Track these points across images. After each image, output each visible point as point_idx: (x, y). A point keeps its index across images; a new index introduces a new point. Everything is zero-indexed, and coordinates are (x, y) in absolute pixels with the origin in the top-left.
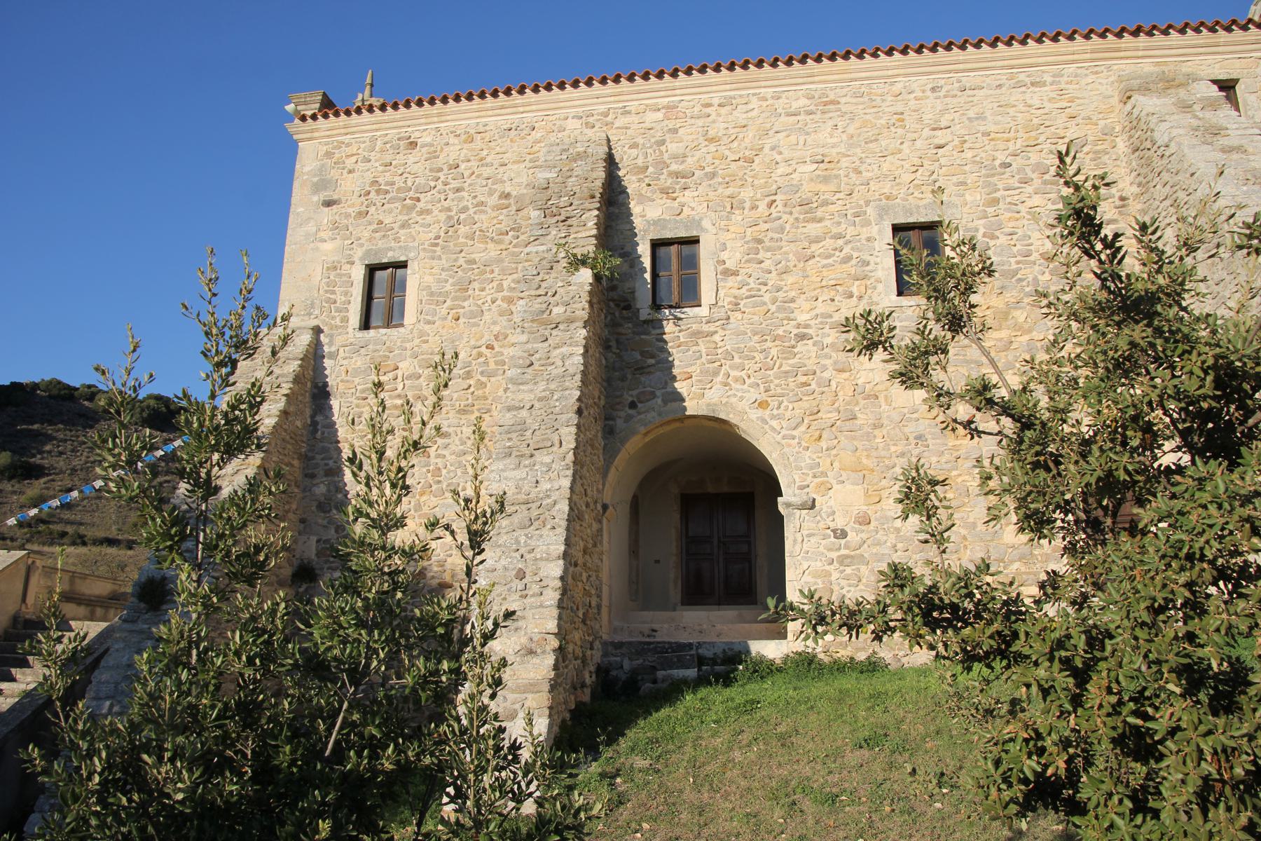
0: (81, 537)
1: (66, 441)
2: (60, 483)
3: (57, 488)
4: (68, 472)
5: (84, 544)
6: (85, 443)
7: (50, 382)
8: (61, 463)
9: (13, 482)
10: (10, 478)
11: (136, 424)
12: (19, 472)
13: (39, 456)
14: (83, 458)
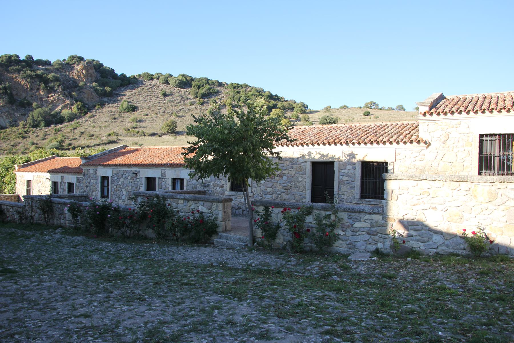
0: (144, 133)
2: (144, 112)
3: (143, 114)
4: (147, 108)
5: (145, 136)
6: (154, 96)
7: (144, 74)
8: (145, 105)
9: (128, 113)
10: (128, 112)
12: (130, 109)
13: (138, 103)
14: (153, 102)
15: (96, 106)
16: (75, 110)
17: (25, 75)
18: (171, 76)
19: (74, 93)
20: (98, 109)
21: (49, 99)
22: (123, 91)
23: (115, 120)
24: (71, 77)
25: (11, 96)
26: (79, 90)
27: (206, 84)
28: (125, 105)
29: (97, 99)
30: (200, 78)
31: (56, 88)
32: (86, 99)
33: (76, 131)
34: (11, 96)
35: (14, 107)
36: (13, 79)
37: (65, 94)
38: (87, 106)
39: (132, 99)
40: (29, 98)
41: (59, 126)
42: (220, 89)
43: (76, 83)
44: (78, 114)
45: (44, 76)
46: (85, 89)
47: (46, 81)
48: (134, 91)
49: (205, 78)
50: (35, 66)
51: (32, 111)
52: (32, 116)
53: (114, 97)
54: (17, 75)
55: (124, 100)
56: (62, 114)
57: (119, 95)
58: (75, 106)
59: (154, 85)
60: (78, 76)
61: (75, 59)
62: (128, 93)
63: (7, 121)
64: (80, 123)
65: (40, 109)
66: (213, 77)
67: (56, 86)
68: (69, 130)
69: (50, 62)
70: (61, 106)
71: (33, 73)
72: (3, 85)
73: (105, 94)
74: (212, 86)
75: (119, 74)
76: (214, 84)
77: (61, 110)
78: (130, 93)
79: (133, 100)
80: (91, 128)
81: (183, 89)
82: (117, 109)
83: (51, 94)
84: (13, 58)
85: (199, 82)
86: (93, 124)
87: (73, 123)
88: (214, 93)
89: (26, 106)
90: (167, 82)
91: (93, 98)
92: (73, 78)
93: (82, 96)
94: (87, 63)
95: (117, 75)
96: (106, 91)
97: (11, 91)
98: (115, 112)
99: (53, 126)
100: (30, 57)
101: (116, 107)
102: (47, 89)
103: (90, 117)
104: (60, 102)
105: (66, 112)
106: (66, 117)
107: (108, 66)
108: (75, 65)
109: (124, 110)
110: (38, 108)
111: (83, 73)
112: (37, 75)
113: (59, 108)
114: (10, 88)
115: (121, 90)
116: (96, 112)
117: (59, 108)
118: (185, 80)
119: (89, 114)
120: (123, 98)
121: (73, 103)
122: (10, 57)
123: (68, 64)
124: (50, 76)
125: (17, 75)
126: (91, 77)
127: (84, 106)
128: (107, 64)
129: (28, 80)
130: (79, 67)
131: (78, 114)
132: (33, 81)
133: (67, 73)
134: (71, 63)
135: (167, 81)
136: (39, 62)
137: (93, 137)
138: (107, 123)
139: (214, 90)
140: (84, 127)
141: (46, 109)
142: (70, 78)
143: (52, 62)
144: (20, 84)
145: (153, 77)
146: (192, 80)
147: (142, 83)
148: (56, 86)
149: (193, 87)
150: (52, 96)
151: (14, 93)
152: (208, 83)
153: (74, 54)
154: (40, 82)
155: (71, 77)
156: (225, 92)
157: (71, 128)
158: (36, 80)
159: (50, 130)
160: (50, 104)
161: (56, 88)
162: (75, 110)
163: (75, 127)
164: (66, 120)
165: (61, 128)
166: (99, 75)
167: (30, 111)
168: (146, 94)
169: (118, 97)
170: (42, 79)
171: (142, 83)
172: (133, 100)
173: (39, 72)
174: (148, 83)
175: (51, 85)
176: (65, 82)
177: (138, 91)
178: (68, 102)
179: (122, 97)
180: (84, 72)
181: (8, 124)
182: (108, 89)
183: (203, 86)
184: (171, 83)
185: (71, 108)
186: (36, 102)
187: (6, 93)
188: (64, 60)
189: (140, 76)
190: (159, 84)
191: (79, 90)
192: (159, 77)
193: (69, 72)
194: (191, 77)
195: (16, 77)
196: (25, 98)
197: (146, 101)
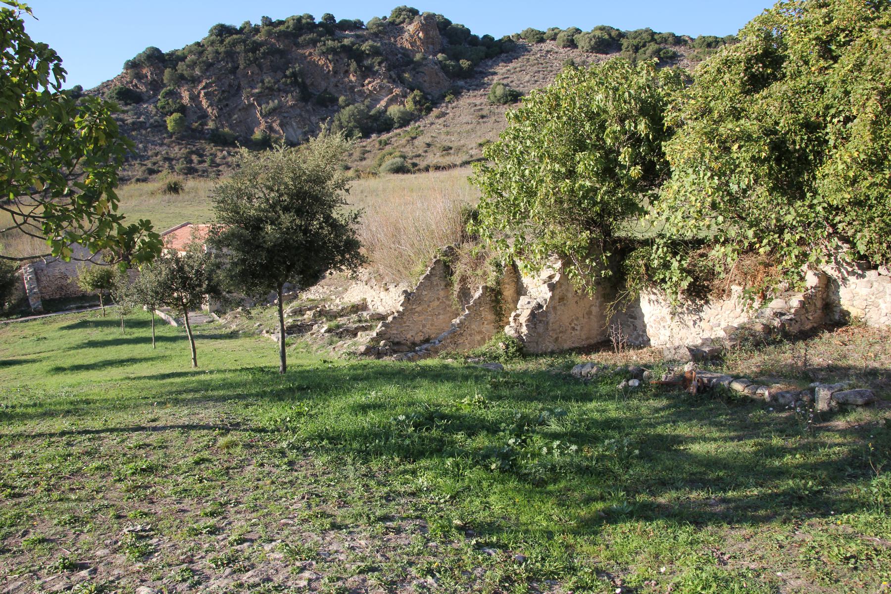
1: (539, 72)
7: (527, 31)
10: (505, 103)
11: (587, 51)
12: (509, 98)
15: (445, 96)
16: (409, 105)
17: (324, 49)
18: (578, 31)
19: (406, 75)
20: (449, 102)
21: (365, 88)
22: (491, 67)
23: (484, 120)
24: (399, 46)
25: (303, 88)
26: (414, 69)
27: (649, 42)
28: (499, 91)
29: (447, 84)
30: (636, 32)
31: (377, 68)
32: (426, 85)
33: (416, 142)
34: (303, 88)
35: (309, 107)
36: (306, 57)
37: (391, 77)
38: (429, 97)
39: (510, 80)
40: (333, 90)
41: (384, 136)
42: (680, 50)
43: (408, 56)
44: (416, 113)
45: (355, 47)
46: (425, 65)
47: (359, 56)
48: (511, 66)
49: (647, 31)
50: (338, 32)
51: (338, 111)
52: (339, 120)
53: (476, 79)
54: (312, 51)
55: (495, 82)
56: (388, 113)
57: (487, 74)
58: (410, 98)
59: (548, 52)
60: (411, 43)
61: (404, 13)
62: (501, 69)
63: (299, 131)
64: (422, 128)
65: (351, 107)
66: (662, 28)
67: (376, 64)
68: (403, 141)
69: (362, 24)
70: (386, 99)
71: (336, 44)
72: (291, 70)
73: (460, 74)
74: (662, 46)
75: (481, 36)
76: (665, 40)
77: (386, 107)
78: (504, 70)
79: (512, 82)
80: (443, 136)
81: (604, 56)
82: (484, 100)
83: (369, 79)
84: (304, 21)
85: (635, 38)
86: (444, 130)
87: (408, 128)
88: (667, 58)
89: (328, 104)
90: (571, 43)
91: (439, 83)
92: (402, 48)
93: (420, 80)
94: (425, 19)
95: (476, 37)
96: (462, 68)
97: (303, 79)
98: (481, 104)
99: (374, 136)
100: (330, 18)
101: (481, 95)
102: (361, 71)
103: (438, 117)
104: (383, 92)
105: (394, 110)
106: (395, 120)
107: (460, 23)
108: (404, 25)
109: (499, 100)
110: (348, 105)
111: (420, 38)
112: (343, 47)
113: (383, 103)
114: (301, 72)
115: (487, 66)
116: (447, 107)
117: (383, 103)
118: (607, 37)
119: (435, 112)
120: (493, 80)
121: (406, 92)
122: (299, 19)
123: (392, 23)
124: (365, 47)
125: (312, 51)
126: (433, 44)
127: (424, 97)
128: (456, 20)
129: (330, 57)
130: (411, 28)
131: (416, 113)
132: (338, 58)
133: (392, 40)
134: (398, 21)
135: (572, 41)
136: (346, 25)
137: (452, 151)
138: (470, 127)
139: (668, 52)
140: (429, 135)
141: (362, 108)
142: (397, 49)
143: (365, 23)
144: (317, 65)
145: (545, 36)
146: (621, 35)
147: (525, 49)
148: (376, 64)
149: (624, 49)
150: (370, 83)
151: (308, 82)
152: (653, 40)
153: (401, 5)
154: (349, 58)
155: (399, 46)
156: (691, 56)
157: (408, 138)
158: (342, 55)
159: (370, 143)
160: (366, 98)
161: (377, 68)
162: (409, 105)
163: (413, 135)
164: (396, 125)
165: (388, 139)
166: (445, 41)
167: (335, 111)
168: (535, 68)
169: (483, 78)
170: (352, 53)
171: (525, 49)
172: (512, 82)
173: (346, 42)
174: (535, 48)
175: (367, 62)
176: (390, 57)
177: (519, 65)
178: (397, 91)
179: (490, 77)
180: (421, 35)
181: (300, 137)
182: (465, 63)
183: (644, 46)
184: (581, 44)
185: (402, 103)
186: (343, 95)
187: (295, 83)
188: (385, 18)
189: (519, 36)
190: (557, 50)
191: (414, 69)
192: (556, 34)
193: (395, 38)
194: (618, 30)
195: (310, 54)
196: (326, 90)
197: (536, 81)
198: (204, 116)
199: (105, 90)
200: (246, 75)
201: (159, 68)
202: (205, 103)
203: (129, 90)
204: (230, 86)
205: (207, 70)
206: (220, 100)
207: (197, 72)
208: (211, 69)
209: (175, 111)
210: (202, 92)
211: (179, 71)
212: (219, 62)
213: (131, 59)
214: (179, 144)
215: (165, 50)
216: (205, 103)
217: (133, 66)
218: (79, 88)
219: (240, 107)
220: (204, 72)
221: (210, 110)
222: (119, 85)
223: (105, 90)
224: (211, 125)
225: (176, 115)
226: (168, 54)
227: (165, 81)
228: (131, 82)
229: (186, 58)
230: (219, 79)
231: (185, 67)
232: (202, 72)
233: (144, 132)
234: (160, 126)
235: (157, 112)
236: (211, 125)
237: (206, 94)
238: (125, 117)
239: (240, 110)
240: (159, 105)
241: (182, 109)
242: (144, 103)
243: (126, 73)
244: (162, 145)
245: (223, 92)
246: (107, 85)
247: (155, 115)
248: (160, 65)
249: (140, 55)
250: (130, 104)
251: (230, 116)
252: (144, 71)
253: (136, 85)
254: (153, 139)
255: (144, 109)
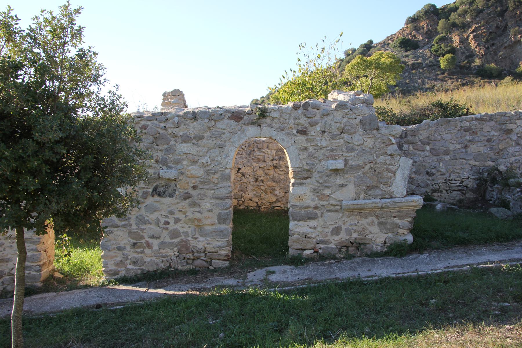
198: (471, 55)
199: (390, 42)
200: (514, 16)
201: (433, 20)
202: (473, 44)
203: (408, 40)
204: (497, 27)
205: (476, 16)
206: (487, 41)
207: (468, 18)
208: (481, 14)
209: (446, 53)
210: (472, 35)
211: (451, 21)
212: (488, 7)
213: (411, 15)
214: (451, 78)
215: (439, 6)
216: (473, 44)
217: (413, 20)
218: (371, 42)
219: (506, 45)
220: (473, 18)
221: (477, 49)
222: (400, 37)
223: (390, 42)
224: (478, 62)
225: (448, 56)
226: (441, 9)
227: (439, 29)
228: (411, 34)
229: (457, 8)
230: (487, 23)
231: (457, 16)
232: (472, 18)
233: (421, 70)
234: (434, 65)
235: (431, 55)
236: (478, 62)
237: (474, 37)
238: (406, 60)
239: (505, 47)
240: (433, 49)
241: (453, 51)
242: (420, 49)
243: (407, 28)
244: (436, 80)
245: (491, 33)
246: (391, 38)
247: (430, 57)
248: (435, 17)
249: (419, 11)
250: (410, 50)
251: (495, 53)
252: (422, 24)
253: (414, 36)
254: (428, 75)
255: (421, 53)
